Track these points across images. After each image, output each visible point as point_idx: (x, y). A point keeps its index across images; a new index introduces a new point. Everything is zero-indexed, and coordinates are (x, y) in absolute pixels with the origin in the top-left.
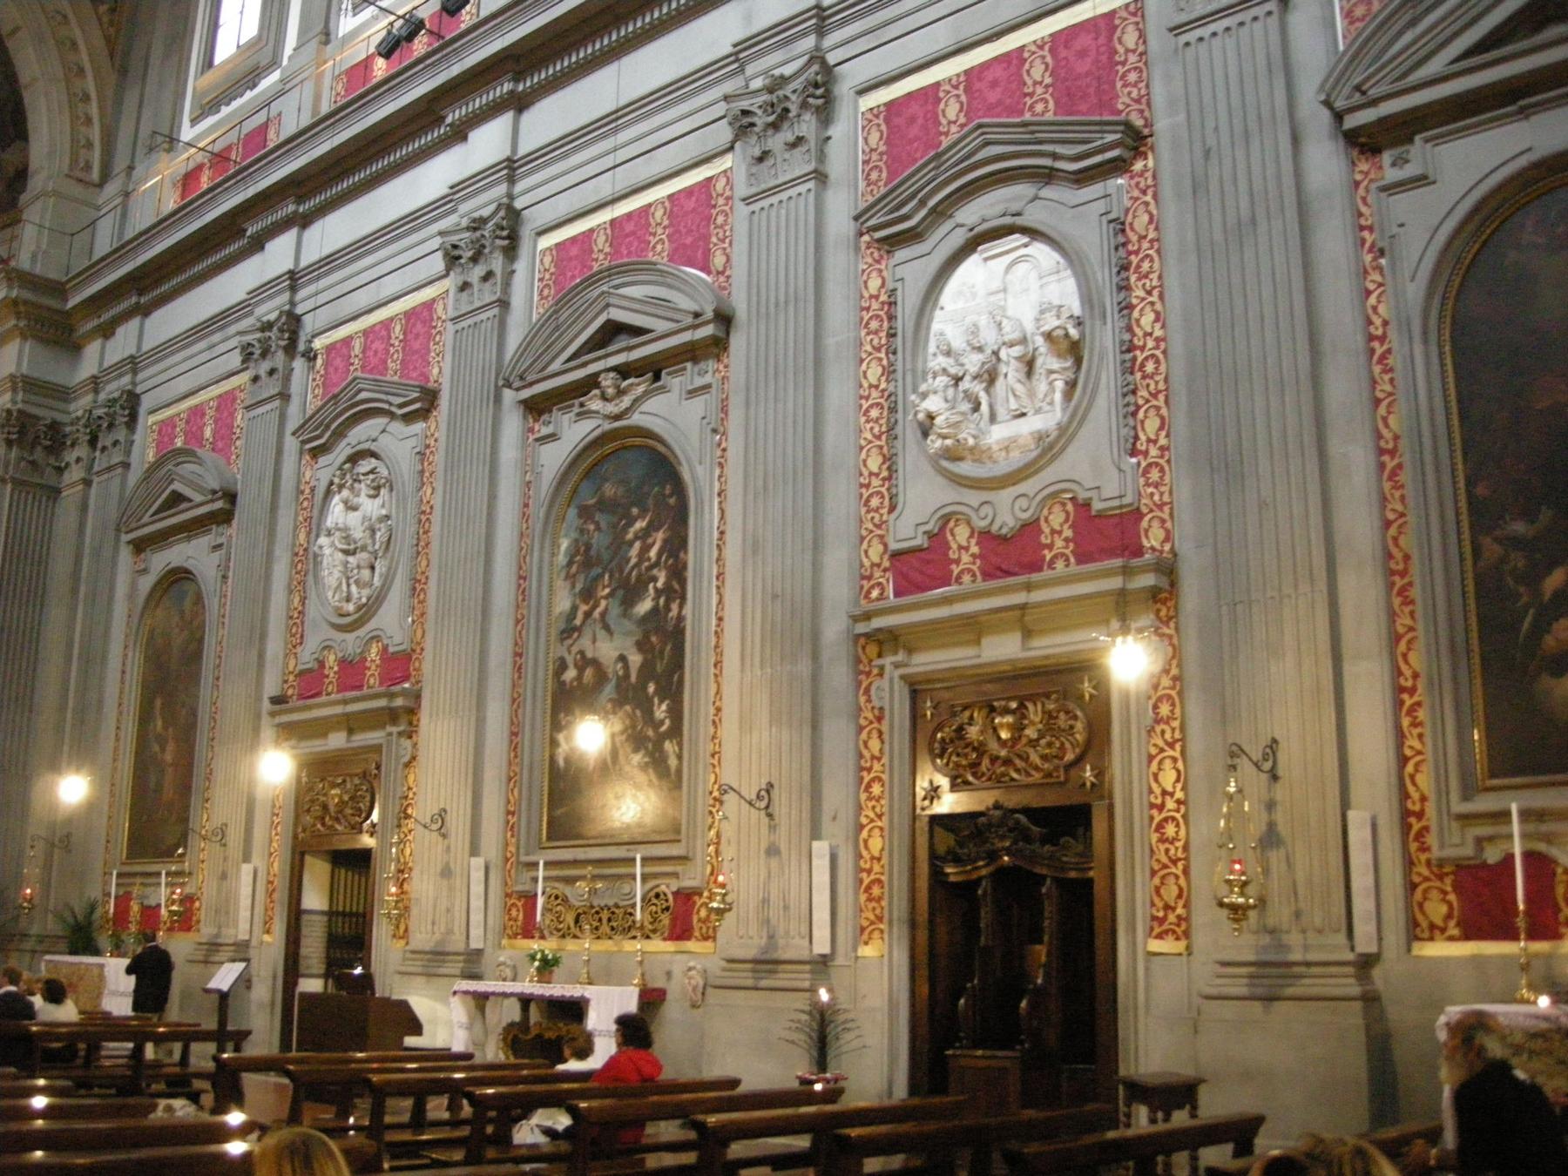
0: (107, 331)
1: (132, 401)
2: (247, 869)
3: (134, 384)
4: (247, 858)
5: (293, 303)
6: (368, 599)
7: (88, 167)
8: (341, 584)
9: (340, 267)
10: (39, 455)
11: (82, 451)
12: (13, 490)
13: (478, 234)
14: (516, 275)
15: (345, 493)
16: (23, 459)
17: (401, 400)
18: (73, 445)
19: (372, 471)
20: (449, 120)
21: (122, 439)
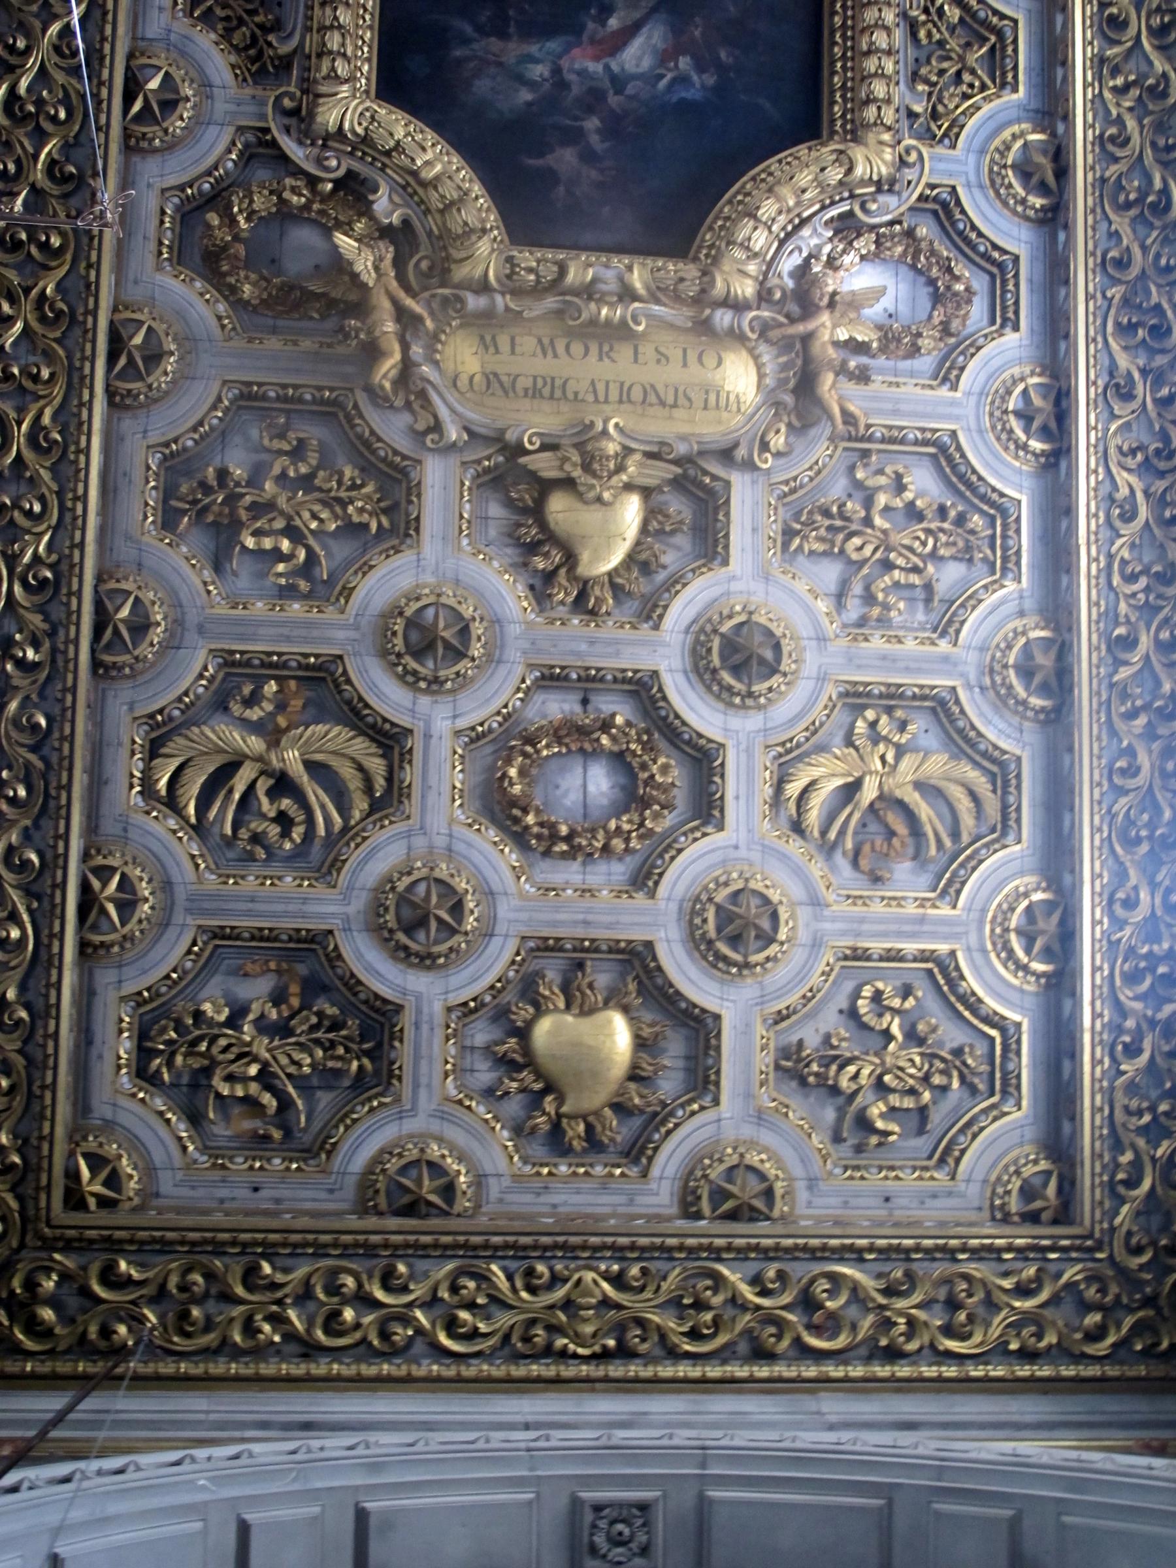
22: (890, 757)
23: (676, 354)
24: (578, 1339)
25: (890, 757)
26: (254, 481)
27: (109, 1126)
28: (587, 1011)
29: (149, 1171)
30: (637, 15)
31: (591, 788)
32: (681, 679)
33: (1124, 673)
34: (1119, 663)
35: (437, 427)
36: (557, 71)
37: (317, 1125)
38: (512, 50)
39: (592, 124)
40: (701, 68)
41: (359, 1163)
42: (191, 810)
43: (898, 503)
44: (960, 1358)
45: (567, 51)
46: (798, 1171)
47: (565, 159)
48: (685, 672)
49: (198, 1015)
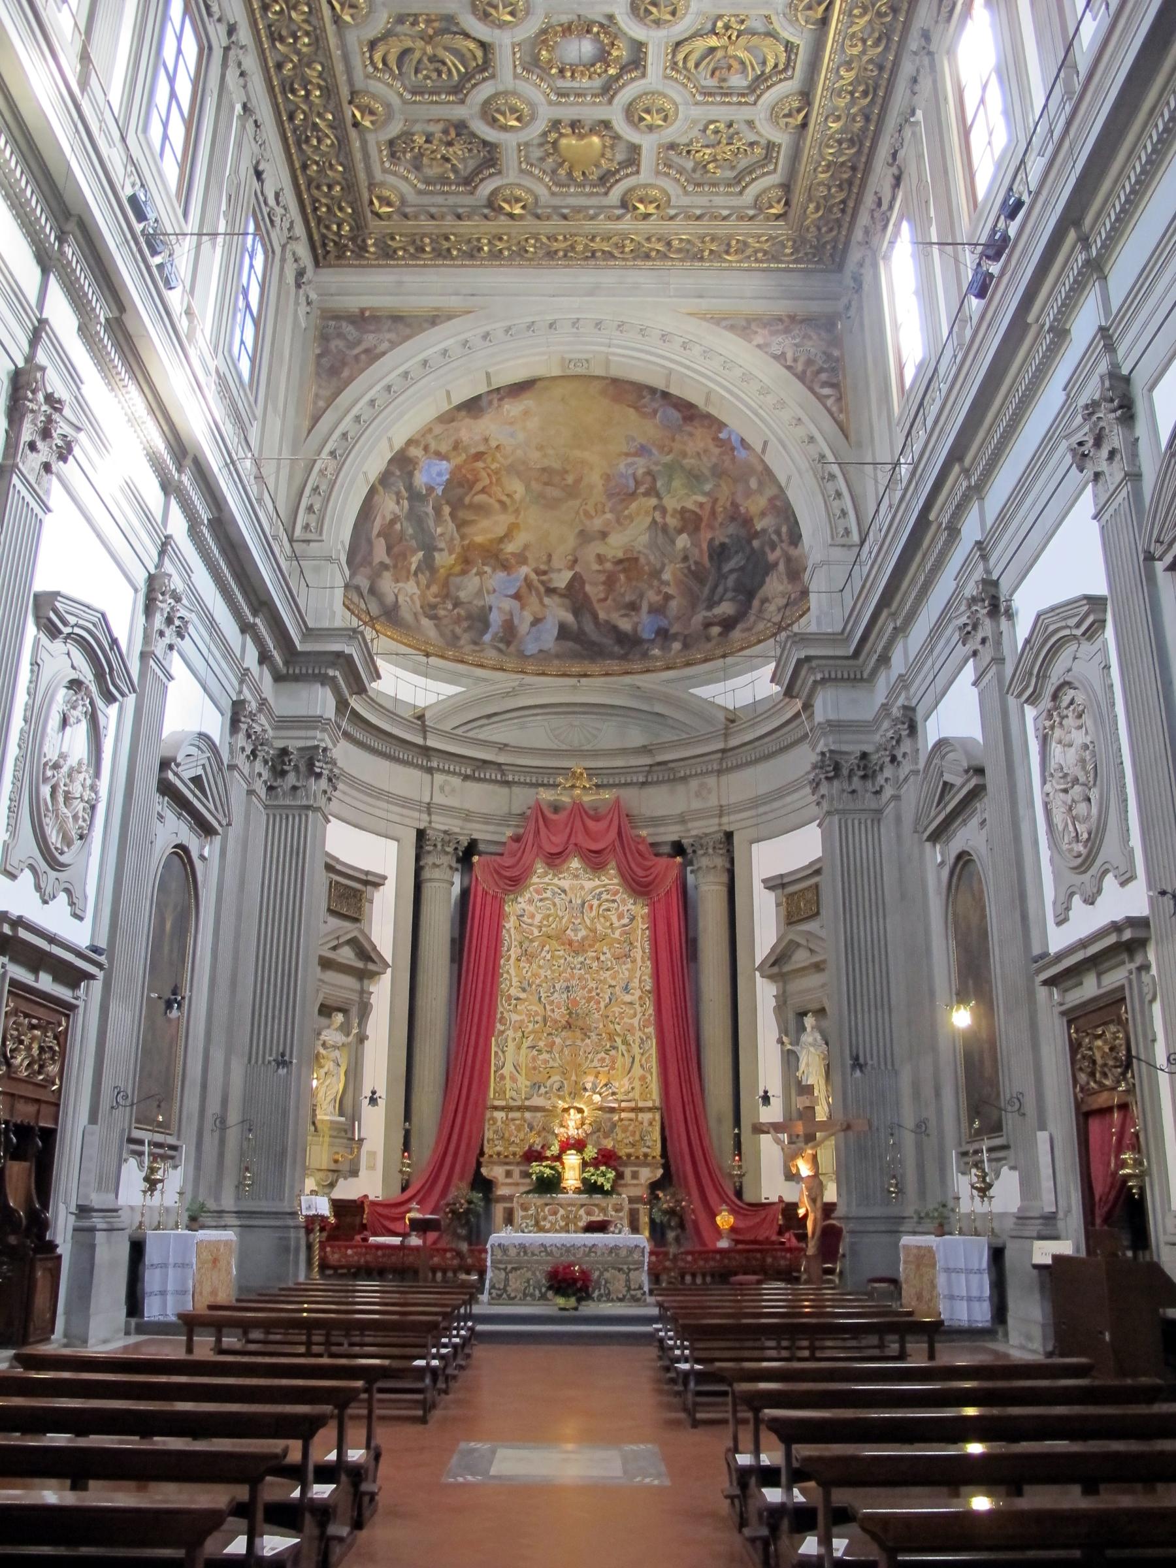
0: (884, 660)
1: (909, 711)
2: (1042, 1137)
3: (907, 698)
4: (1043, 1127)
5: (988, 572)
6: (1090, 834)
7: (847, 532)
8: (1067, 825)
9: (1012, 517)
10: (856, 783)
11: (888, 772)
12: (840, 820)
13: (1094, 418)
14: (1140, 442)
15: (1058, 733)
16: (843, 791)
17: (1076, 620)
18: (881, 769)
19: (1072, 702)
21: (908, 751)
22: (734, 38)
24: (576, 253)
25: (734, 38)
27: (382, 184)
28: (581, 137)
31: (583, 50)
32: (625, 17)
33: (855, 29)
34: (853, 23)
37: (469, 170)
42: (395, 68)
44: (731, 262)
46: (671, 191)
49: (413, 142)
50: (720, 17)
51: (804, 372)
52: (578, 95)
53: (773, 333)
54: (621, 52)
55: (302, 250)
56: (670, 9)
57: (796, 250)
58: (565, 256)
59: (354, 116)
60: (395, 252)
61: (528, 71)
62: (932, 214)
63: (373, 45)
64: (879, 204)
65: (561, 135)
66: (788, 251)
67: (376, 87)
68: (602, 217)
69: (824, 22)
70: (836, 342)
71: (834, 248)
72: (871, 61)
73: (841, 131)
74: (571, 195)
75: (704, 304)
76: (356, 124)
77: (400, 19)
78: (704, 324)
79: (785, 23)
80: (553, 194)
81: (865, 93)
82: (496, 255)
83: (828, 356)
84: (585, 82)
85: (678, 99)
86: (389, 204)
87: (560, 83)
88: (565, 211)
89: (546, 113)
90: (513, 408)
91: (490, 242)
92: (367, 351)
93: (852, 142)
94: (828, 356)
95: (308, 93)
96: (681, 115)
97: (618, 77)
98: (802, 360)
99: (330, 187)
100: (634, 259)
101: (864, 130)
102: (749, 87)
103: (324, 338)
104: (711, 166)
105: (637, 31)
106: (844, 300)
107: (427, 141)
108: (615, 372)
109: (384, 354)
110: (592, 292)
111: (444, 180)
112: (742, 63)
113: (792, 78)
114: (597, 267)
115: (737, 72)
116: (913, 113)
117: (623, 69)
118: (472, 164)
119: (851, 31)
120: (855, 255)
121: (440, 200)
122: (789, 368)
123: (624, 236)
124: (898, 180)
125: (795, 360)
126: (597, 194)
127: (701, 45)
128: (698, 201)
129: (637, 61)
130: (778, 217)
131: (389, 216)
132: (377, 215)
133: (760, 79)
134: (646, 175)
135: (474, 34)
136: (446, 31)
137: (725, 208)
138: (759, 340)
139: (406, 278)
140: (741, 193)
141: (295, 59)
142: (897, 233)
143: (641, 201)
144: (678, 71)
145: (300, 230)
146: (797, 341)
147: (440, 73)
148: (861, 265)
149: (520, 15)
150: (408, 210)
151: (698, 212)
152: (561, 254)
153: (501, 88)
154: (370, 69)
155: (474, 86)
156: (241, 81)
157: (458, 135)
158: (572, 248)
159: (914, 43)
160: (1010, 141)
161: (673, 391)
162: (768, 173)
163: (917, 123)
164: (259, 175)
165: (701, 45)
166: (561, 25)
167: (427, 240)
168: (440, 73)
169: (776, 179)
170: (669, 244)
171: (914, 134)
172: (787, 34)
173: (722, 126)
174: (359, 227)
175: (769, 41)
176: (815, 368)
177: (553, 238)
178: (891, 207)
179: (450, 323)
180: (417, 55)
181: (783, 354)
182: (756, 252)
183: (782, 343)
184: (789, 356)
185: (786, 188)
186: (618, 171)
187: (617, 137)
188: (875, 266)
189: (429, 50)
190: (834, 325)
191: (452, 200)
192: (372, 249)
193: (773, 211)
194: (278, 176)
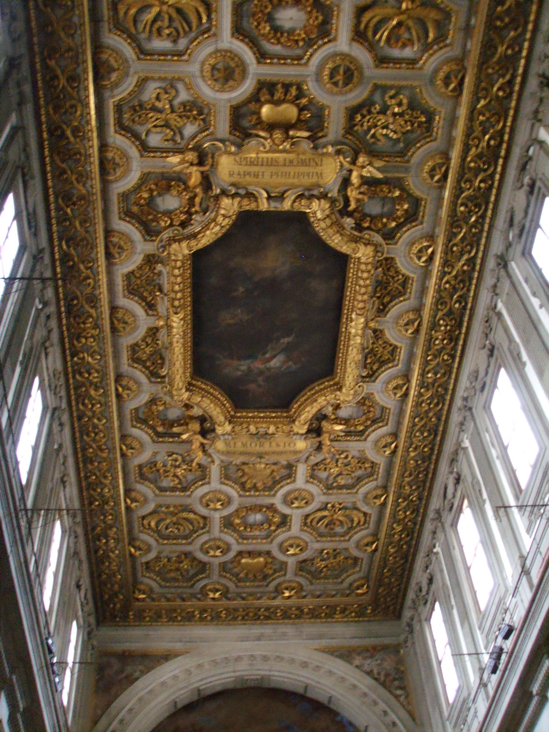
20: (534, 692)
23: (282, 444)
26: (165, 466)
27: (141, 583)
28: (253, 558)
29: (151, 590)
30: (274, 353)
35: (213, 462)
36: (249, 368)
38: (235, 363)
39: (260, 379)
40: (295, 364)
41: (200, 586)
43: (345, 461)
45: (252, 362)
47: (252, 387)
48: (282, 503)
50: (330, 503)
51: (384, 681)
52: (253, 539)
53: (365, 658)
54: (277, 519)
55: (92, 620)
56: (305, 501)
57: (373, 610)
58: (243, 619)
59: (130, 551)
60: (145, 618)
61: (228, 528)
62: (453, 603)
63: (143, 518)
64: (420, 590)
65: (243, 558)
66: (369, 611)
67: (144, 537)
68: (265, 598)
69: (384, 504)
70: (400, 661)
71: (395, 608)
72: (409, 521)
73: (396, 552)
74: (248, 587)
75: (324, 643)
76: (131, 555)
77: (160, 506)
78: (325, 655)
79: (364, 504)
80: (237, 586)
81: (408, 535)
82: (202, 619)
83: (398, 670)
84: (257, 533)
85: (308, 540)
86: (144, 593)
87: (245, 533)
88: (244, 595)
89: (236, 548)
90: (211, 706)
91: (201, 613)
92: (127, 677)
93: (402, 558)
94: (398, 670)
95: (107, 541)
96: (309, 547)
97: (275, 531)
98: (383, 673)
99: (113, 585)
100: (283, 619)
101: (408, 551)
102: (344, 532)
103: (101, 669)
104: (324, 569)
105: (286, 510)
106: (403, 637)
107: (169, 560)
108: (272, 685)
109: (137, 679)
110: (259, 638)
111: (176, 580)
112: (341, 522)
113: (368, 528)
114: (261, 624)
115: (338, 526)
116: (434, 547)
117: (278, 527)
118: (192, 572)
119: (398, 509)
120: (407, 614)
121: (173, 590)
122: (376, 679)
123: (277, 607)
124: (431, 581)
125: (379, 674)
126: (261, 586)
127: (320, 514)
128: (318, 587)
129: (285, 520)
130: (362, 594)
131: (143, 600)
132: (138, 600)
133: (351, 528)
134: (289, 576)
135: (200, 513)
136: (183, 511)
137: (334, 590)
138: (357, 662)
139: (151, 633)
140: (342, 582)
141: (103, 525)
142: (433, 609)
143: (287, 589)
144: (308, 527)
145: (93, 610)
146: (379, 662)
147: (179, 530)
148: (412, 619)
149: (225, 505)
150: (154, 596)
151: (318, 593)
152: (240, 618)
153: (212, 537)
154: (142, 528)
155: (198, 536)
156: (75, 540)
157: (186, 558)
158: (247, 614)
159: (431, 514)
160: (495, 584)
161: (309, 695)
162: (356, 572)
163: (437, 553)
164: (78, 586)
165: (320, 514)
166: (246, 507)
167: (163, 612)
168: (179, 530)
169: (361, 574)
170: (302, 611)
171: (437, 558)
172: (365, 509)
173: (331, 551)
174: (126, 607)
175: (355, 512)
176: (391, 678)
177: (236, 610)
178: (428, 593)
179: (176, 660)
180: (168, 521)
181: (372, 671)
182: (351, 613)
183: (370, 664)
184: (375, 671)
185: (367, 578)
186: (273, 574)
187: (274, 558)
188: (420, 621)
189: (174, 519)
190: (398, 652)
191: (180, 590)
192: (132, 617)
193: (360, 591)
194: (86, 582)
